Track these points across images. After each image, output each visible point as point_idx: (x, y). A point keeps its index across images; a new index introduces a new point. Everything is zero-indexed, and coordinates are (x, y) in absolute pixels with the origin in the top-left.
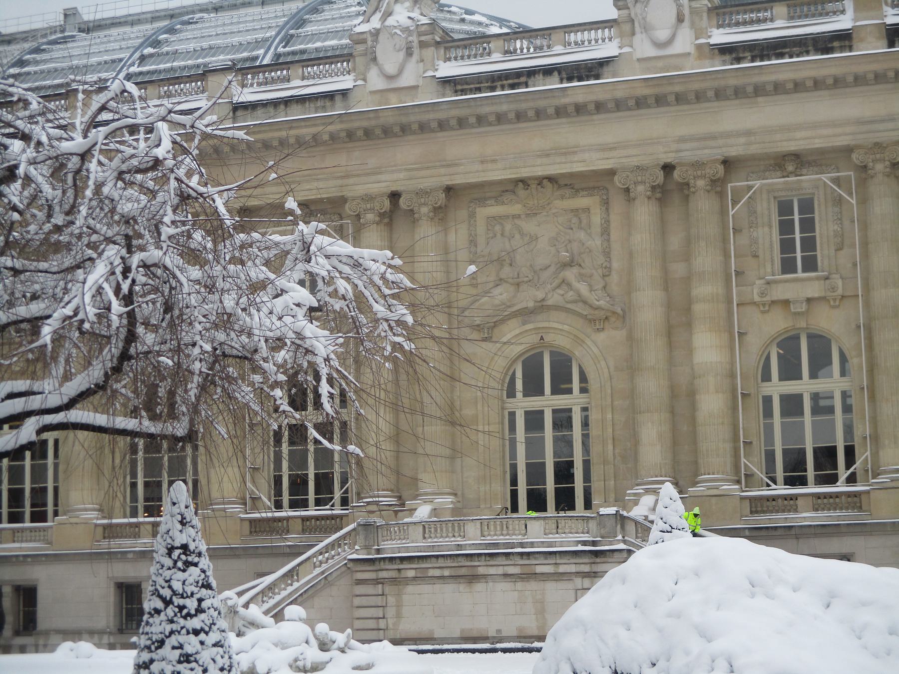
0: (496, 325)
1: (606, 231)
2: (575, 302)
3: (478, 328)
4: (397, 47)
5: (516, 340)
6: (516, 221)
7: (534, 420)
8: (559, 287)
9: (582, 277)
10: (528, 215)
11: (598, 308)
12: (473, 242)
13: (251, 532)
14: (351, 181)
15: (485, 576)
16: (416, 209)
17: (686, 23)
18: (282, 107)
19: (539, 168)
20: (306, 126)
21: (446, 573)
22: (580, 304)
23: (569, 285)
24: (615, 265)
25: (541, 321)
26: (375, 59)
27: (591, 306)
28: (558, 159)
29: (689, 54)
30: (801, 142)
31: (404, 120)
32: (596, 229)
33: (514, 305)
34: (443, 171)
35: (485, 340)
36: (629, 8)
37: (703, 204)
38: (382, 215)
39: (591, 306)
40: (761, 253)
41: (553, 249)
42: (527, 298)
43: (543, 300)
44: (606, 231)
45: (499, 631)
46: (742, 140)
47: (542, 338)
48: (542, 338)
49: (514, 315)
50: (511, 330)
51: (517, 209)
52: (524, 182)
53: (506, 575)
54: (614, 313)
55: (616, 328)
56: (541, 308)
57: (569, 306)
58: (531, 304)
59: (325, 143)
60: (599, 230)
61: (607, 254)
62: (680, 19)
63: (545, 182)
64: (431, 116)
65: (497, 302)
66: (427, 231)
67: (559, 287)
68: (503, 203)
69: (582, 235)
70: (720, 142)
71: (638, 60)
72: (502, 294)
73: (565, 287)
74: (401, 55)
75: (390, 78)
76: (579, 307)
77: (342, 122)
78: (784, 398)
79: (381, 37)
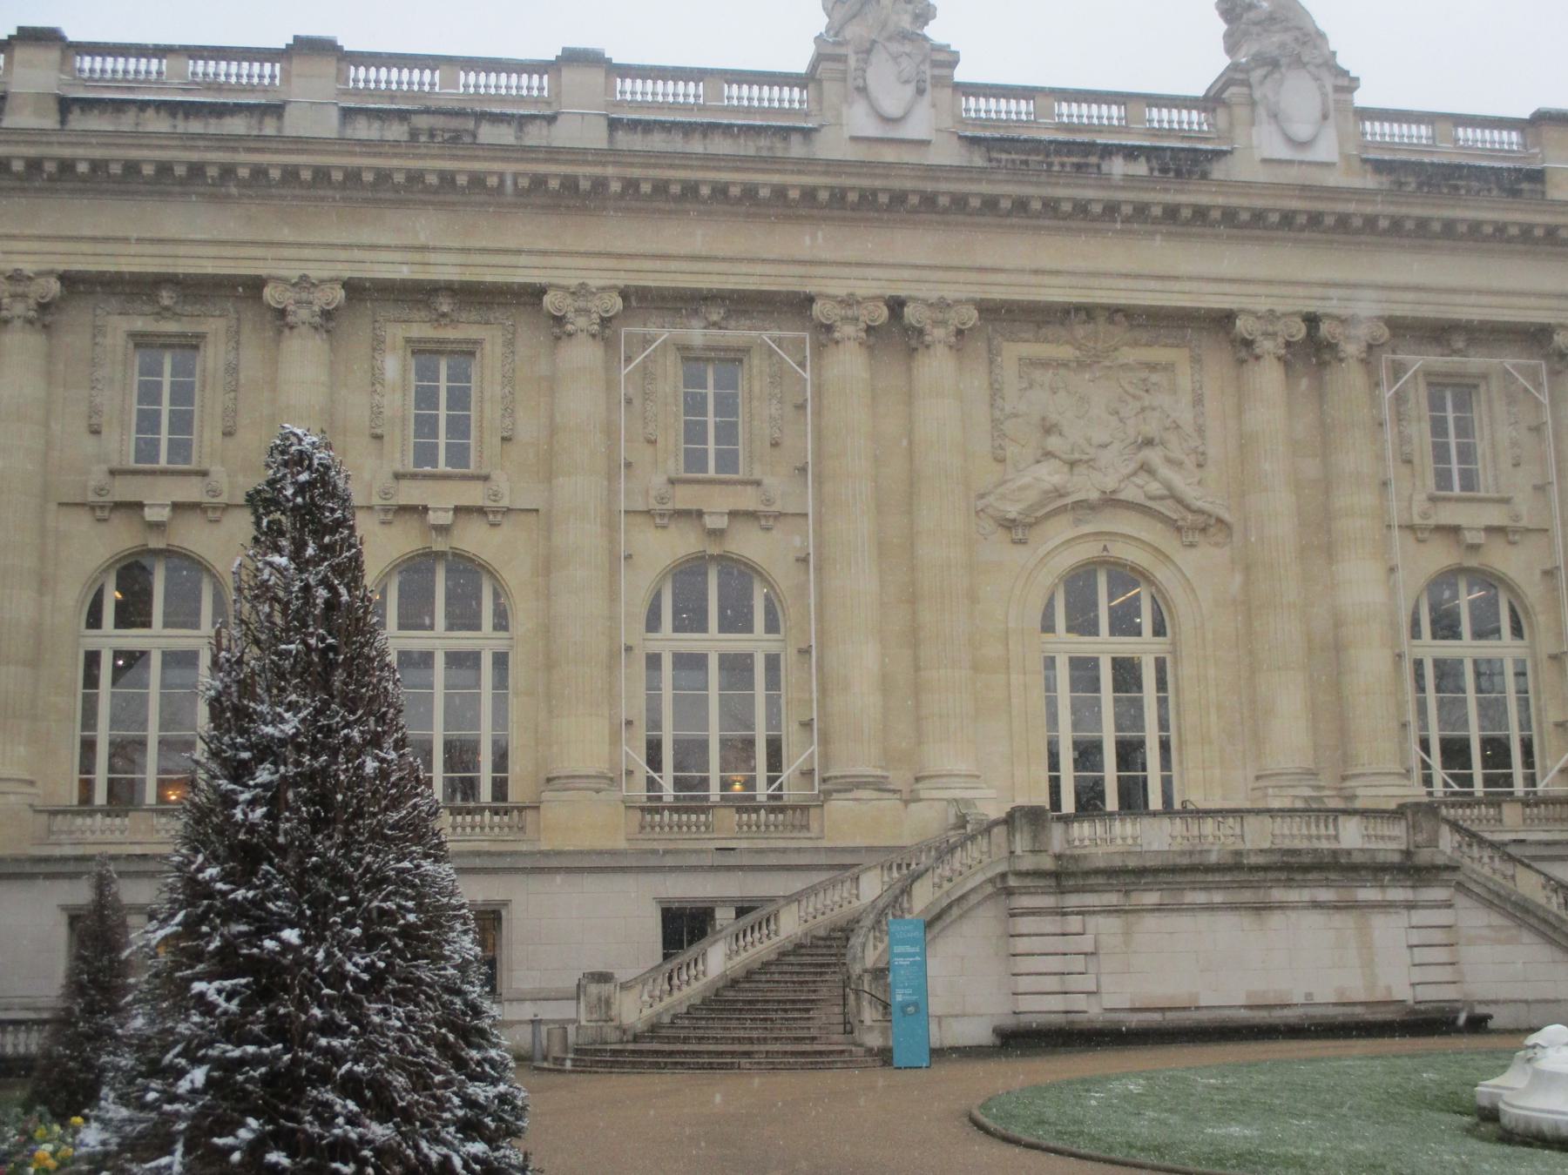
0: (1038, 521)
1: (1198, 401)
2: (1162, 498)
5: (1063, 547)
6: (1062, 371)
7: (1084, 671)
8: (1135, 473)
9: (1170, 461)
10: (1081, 365)
11: (1201, 512)
12: (996, 392)
14: (822, 271)
17: (1331, 120)
18: (697, 136)
19: (1123, 294)
22: (1170, 502)
24: (1213, 451)
26: (863, 90)
27: (1188, 508)
28: (1152, 284)
29: (1333, 164)
31: (929, 187)
34: (973, 276)
35: (1022, 542)
36: (1250, 86)
37: (1349, 379)
38: (869, 330)
40: (1416, 460)
41: (1114, 420)
42: (1087, 486)
44: (1198, 401)
45: (1309, 995)
46: (1410, 296)
47: (1105, 548)
48: (1105, 548)
49: (1063, 509)
50: (1060, 530)
51: (1066, 352)
52: (1087, 312)
54: (1220, 521)
55: (1217, 544)
56: (1111, 502)
58: (1094, 495)
61: (1200, 430)
62: (1325, 117)
65: (1047, 486)
66: (937, 366)
67: (1135, 473)
68: (1046, 340)
71: (1265, 161)
72: (1050, 475)
74: (910, 90)
75: (888, 120)
77: (826, 173)
78: (1439, 664)
79: (874, 58)
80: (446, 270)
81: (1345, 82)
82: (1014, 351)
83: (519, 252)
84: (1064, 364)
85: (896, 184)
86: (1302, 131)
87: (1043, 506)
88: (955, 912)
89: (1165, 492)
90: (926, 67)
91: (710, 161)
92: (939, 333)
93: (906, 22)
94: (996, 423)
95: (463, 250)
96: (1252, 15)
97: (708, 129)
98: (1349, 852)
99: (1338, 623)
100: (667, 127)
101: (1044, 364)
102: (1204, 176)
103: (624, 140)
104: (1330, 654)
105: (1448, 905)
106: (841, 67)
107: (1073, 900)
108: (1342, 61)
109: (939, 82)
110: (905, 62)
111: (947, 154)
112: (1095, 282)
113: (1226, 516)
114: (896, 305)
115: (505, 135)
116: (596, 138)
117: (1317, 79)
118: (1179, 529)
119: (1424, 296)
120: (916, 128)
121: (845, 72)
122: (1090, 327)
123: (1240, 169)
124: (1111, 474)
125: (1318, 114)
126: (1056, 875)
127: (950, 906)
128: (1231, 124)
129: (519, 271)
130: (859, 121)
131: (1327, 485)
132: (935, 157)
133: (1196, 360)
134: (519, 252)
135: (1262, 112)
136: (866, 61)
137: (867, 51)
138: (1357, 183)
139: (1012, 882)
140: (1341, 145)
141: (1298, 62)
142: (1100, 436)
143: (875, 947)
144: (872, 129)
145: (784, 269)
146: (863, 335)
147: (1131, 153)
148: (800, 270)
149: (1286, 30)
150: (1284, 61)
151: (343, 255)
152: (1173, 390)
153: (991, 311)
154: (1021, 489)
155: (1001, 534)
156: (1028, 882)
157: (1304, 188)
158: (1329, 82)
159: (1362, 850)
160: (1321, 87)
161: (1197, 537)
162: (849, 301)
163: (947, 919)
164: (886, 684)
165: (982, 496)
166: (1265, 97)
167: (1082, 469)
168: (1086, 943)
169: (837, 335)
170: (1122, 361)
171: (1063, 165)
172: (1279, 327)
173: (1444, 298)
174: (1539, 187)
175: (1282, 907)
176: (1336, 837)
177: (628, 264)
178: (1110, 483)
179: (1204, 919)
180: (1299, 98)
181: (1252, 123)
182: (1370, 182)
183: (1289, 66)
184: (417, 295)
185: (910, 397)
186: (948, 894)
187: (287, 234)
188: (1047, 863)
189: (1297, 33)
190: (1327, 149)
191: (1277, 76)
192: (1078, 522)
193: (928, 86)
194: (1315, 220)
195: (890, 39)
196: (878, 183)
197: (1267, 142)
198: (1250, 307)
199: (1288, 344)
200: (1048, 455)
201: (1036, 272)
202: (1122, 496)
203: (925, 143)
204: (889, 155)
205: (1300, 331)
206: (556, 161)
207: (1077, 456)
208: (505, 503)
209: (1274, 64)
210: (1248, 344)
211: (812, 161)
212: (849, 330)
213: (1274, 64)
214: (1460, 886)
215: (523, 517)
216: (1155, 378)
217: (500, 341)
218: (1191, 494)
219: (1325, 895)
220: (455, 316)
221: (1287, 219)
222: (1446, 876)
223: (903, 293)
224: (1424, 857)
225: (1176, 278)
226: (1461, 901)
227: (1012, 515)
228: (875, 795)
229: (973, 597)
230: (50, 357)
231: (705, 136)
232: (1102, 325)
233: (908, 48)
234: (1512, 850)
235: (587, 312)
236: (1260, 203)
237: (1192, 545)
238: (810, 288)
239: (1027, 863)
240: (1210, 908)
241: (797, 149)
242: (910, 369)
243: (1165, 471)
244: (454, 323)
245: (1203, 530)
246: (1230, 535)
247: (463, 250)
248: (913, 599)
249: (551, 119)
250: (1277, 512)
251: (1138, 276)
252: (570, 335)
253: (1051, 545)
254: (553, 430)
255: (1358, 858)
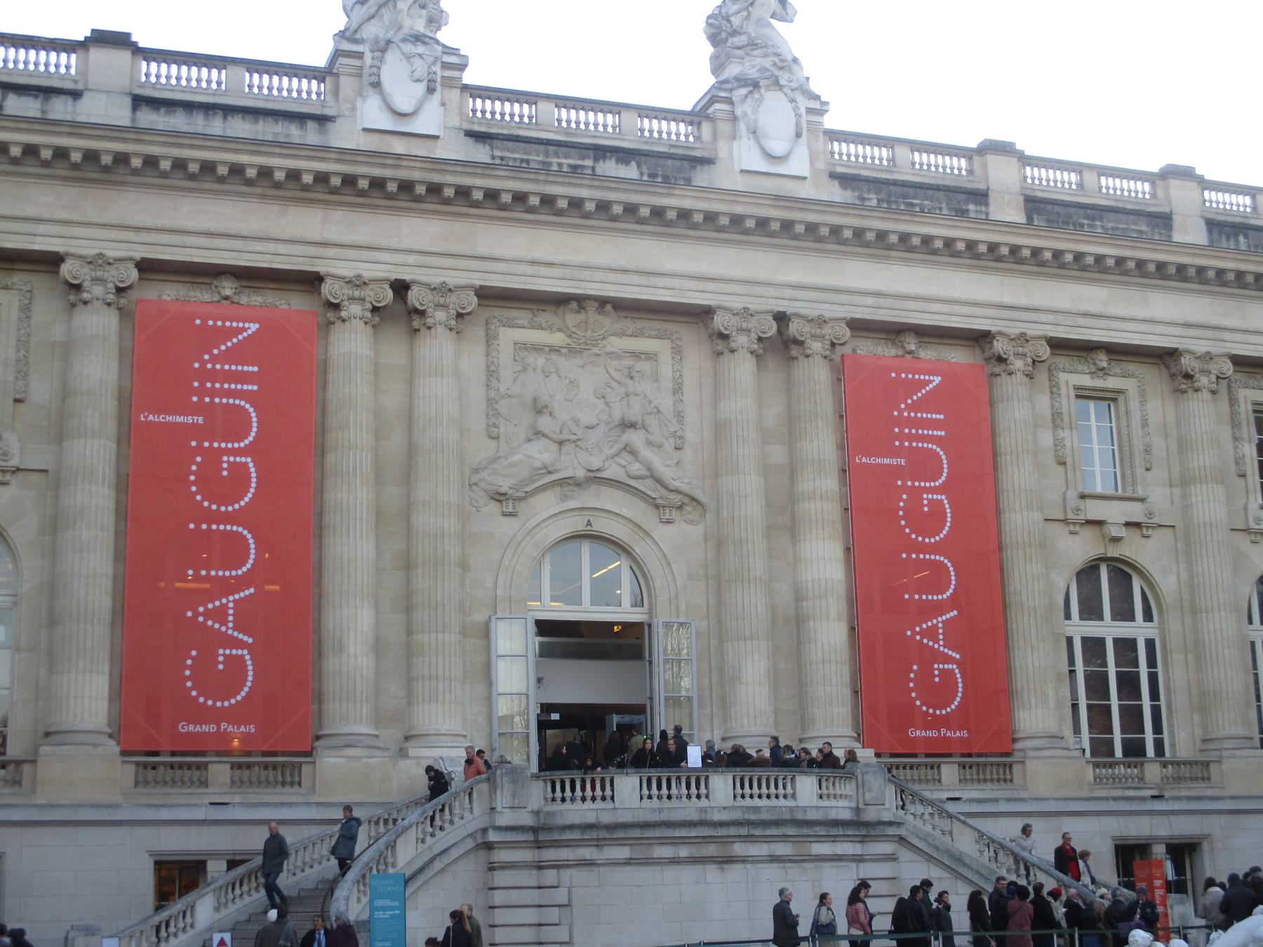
1: (678, 389)
3: (499, 497)
4: (417, 75)
6: (554, 357)
8: (618, 454)
9: (649, 443)
10: (572, 352)
11: (678, 492)
13: (137, 783)
14: (331, 252)
15: (744, 860)
16: (430, 310)
20: (281, 155)
21: (684, 852)
22: (649, 482)
23: (633, 453)
24: (689, 436)
25: (588, 498)
26: (377, 85)
27: (666, 487)
29: (805, 178)
30: (936, 317)
31: (436, 178)
32: (668, 385)
33: (557, 471)
35: (511, 515)
38: (375, 310)
39: (666, 487)
41: (600, 403)
42: (573, 464)
43: (598, 470)
44: (678, 389)
46: (870, 301)
50: (547, 504)
51: (557, 339)
52: (580, 301)
53: (774, 859)
54: (693, 499)
55: (691, 522)
56: (595, 479)
57: (632, 482)
58: (581, 474)
59: (278, 185)
60: (670, 386)
61: (680, 417)
62: (798, 135)
63: (609, 307)
64: (478, 182)
65: (537, 464)
66: (437, 346)
67: (618, 454)
68: (540, 328)
69: (647, 387)
70: (845, 298)
72: (541, 453)
73: (628, 457)
74: (421, 88)
76: (646, 486)
77: (339, 161)
81: (818, 106)
82: (508, 337)
83: (39, 220)
84: (554, 350)
85: (403, 174)
86: (778, 148)
87: (533, 482)
88: (438, 865)
89: (645, 472)
90: (437, 68)
91: (226, 141)
92: (441, 315)
93: (420, 26)
94: (491, 402)
96: (737, 40)
97: (228, 111)
98: (804, 809)
99: (799, 597)
100: (189, 106)
101: (537, 348)
102: (688, 181)
103: (148, 118)
104: (792, 626)
105: (892, 858)
106: (357, 63)
107: (550, 854)
108: (814, 87)
109: (449, 83)
110: (418, 62)
111: (454, 149)
112: (585, 274)
113: (700, 497)
114: (400, 288)
115: (28, 107)
116: (120, 114)
117: (792, 101)
118: (657, 506)
119: (882, 301)
120: (427, 122)
121: (361, 68)
122: (582, 317)
123: (725, 177)
124: (596, 455)
125: (792, 133)
126: (534, 830)
127: (432, 860)
128: (715, 137)
129: (39, 239)
130: (372, 113)
131: (792, 469)
132: (441, 152)
133: (677, 351)
134: (39, 220)
135: (742, 127)
136: (381, 60)
137: (382, 48)
138: (825, 197)
139: (493, 836)
140: (812, 163)
141: (777, 84)
142: (587, 417)
143: (359, 900)
144: (385, 123)
145: (296, 249)
146: (369, 315)
147: (624, 155)
148: (311, 250)
149: (766, 56)
150: (762, 83)
152: (656, 378)
153: (487, 295)
154: (512, 465)
155: (493, 507)
156: (508, 837)
157: (778, 198)
158: (803, 103)
159: (817, 808)
160: (796, 109)
161: (675, 515)
162: (358, 283)
163: (429, 873)
164: (379, 647)
165: (476, 471)
166: (745, 114)
167: (568, 448)
168: (560, 896)
169: (343, 314)
170: (609, 349)
171: (560, 165)
172: (752, 323)
173: (898, 304)
174: (983, 208)
175: (744, 860)
176: (794, 796)
177: (146, 237)
178: (595, 463)
179: (671, 872)
180: (775, 115)
181: (734, 139)
182: (835, 193)
183: (768, 87)
185: (411, 376)
186: (430, 848)
188: (526, 819)
189: (776, 59)
190: (799, 165)
191: (756, 96)
192: (565, 498)
193: (439, 88)
194: (787, 225)
195: (404, 40)
196: (388, 173)
197: (745, 155)
198: (727, 304)
199: (760, 339)
200: (538, 434)
201: (533, 263)
202: (605, 474)
203: (437, 137)
204: (399, 146)
205: (771, 329)
206: (80, 136)
207: (565, 436)
208: (15, 462)
209: (756, 85)
210: (723, 337)
211: (327, 149)
212: (355, 309)
213: (756, 85)
214: (902, 840)
215: (33, 477)
216: (639, 366)
217: (16, 305)
218: (668, 474)
219: (782, 849)
221: (763, 223)
222: (892, 831)
223: (407, 277)
224: (871, 815)
225: (662, 275)
226: (904, 854)
227: (503, 490)
228: (364, 752)
229: (464, 565)
231: (225, 117)
232: (591, 315)
233: (421, 49)
234: (951, 807)
235: (103, 281)
236: (739, 209)
237: (669, 522)
238: (320, 268)
239: (506, 819)
240: (675, 861)
241: (311, 135)
242: (411, 348)
243: (647, 454)
245: (680, 508)
246: (703, 514)
248: (408, 564)
250: (748, 495)
251: (625, 271)
252: (85, 303)
253: (538, 519)
254: (65, 392)
255: (812, 815)
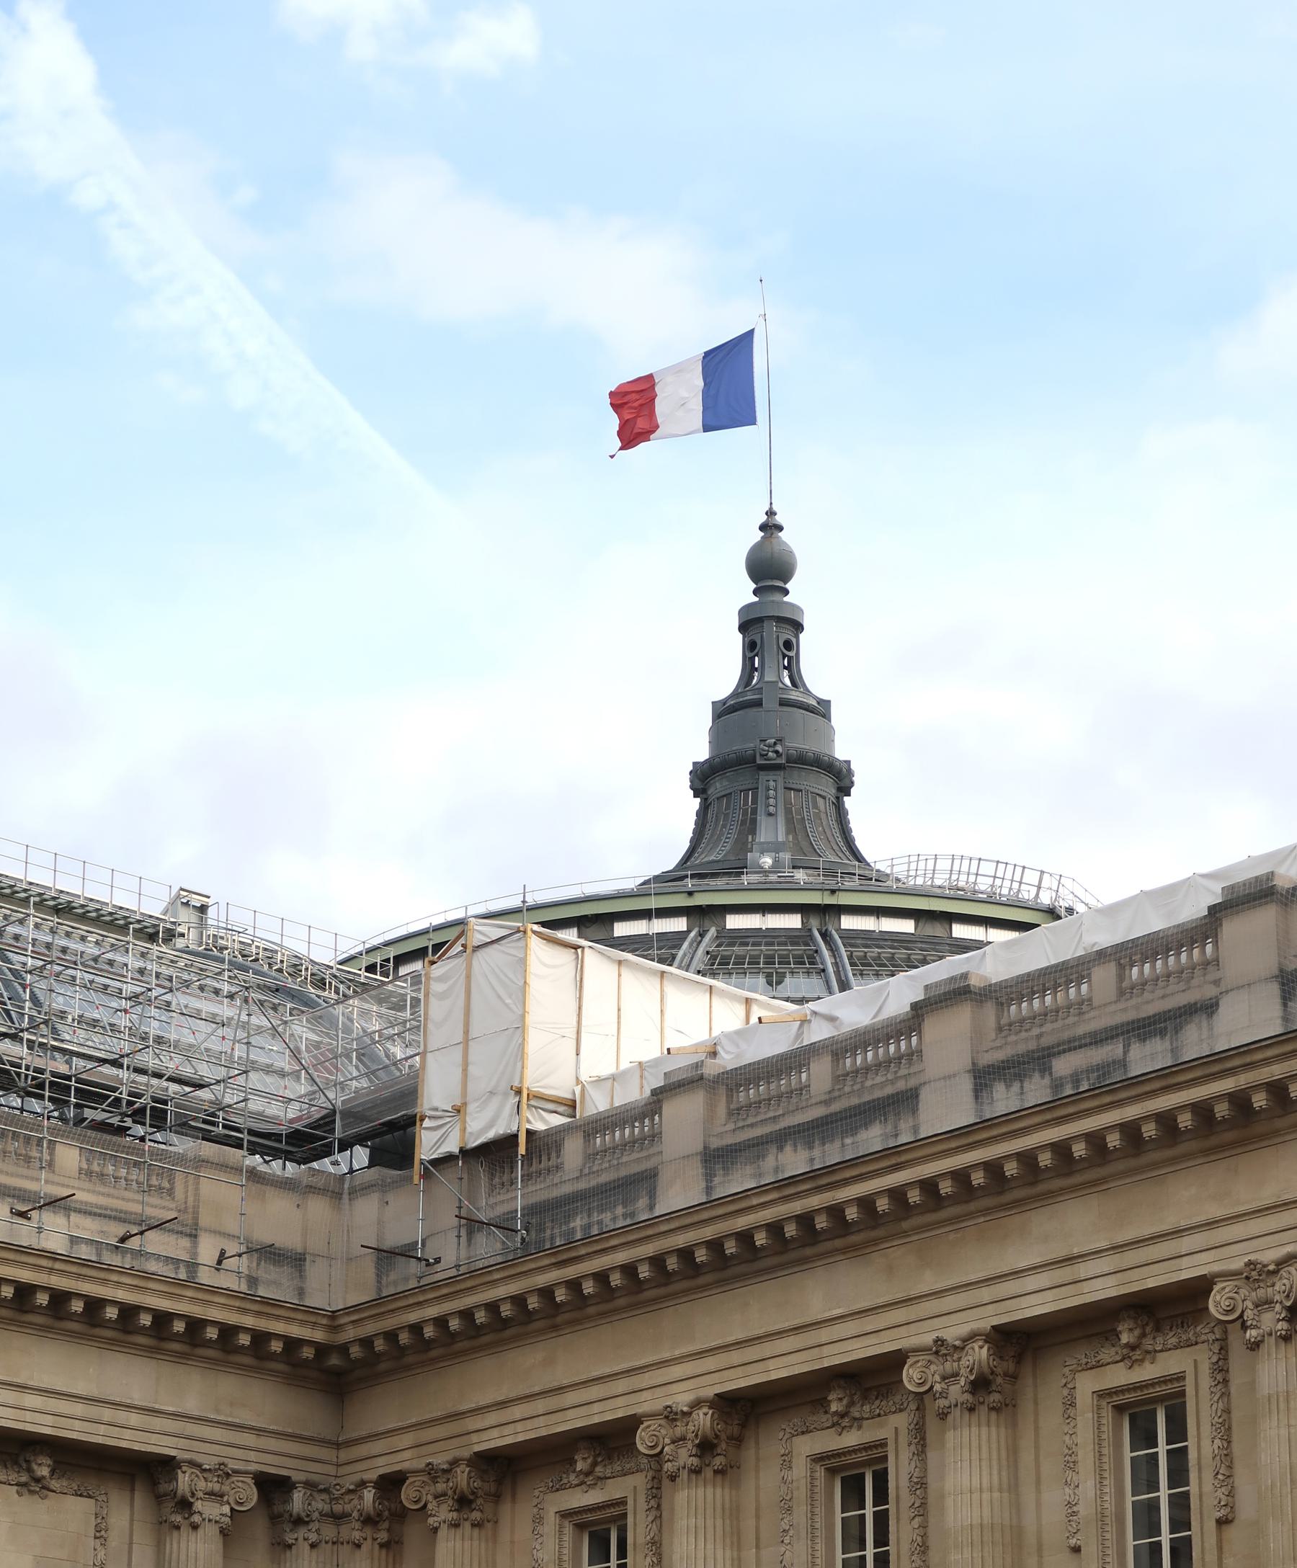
80: (1101, 1285)
95: (1117, 1248)
129: (1185, 1262)
151: (985, 1294)
184: (1087, 1326)
187: (929, 1281)
217: (1205, 1368)
220: (1148, 1343)
230: (733, 1513)
244: (1152, 1354)
247: (1117, 1248)
249: (1209, 1008)
